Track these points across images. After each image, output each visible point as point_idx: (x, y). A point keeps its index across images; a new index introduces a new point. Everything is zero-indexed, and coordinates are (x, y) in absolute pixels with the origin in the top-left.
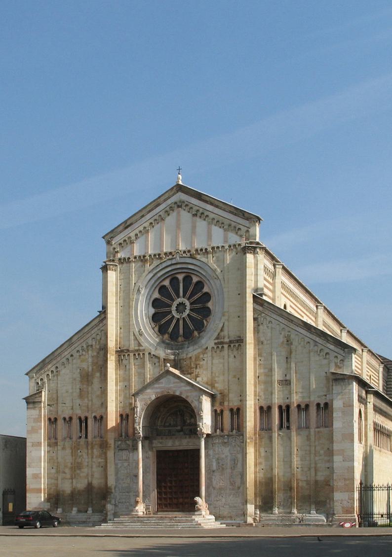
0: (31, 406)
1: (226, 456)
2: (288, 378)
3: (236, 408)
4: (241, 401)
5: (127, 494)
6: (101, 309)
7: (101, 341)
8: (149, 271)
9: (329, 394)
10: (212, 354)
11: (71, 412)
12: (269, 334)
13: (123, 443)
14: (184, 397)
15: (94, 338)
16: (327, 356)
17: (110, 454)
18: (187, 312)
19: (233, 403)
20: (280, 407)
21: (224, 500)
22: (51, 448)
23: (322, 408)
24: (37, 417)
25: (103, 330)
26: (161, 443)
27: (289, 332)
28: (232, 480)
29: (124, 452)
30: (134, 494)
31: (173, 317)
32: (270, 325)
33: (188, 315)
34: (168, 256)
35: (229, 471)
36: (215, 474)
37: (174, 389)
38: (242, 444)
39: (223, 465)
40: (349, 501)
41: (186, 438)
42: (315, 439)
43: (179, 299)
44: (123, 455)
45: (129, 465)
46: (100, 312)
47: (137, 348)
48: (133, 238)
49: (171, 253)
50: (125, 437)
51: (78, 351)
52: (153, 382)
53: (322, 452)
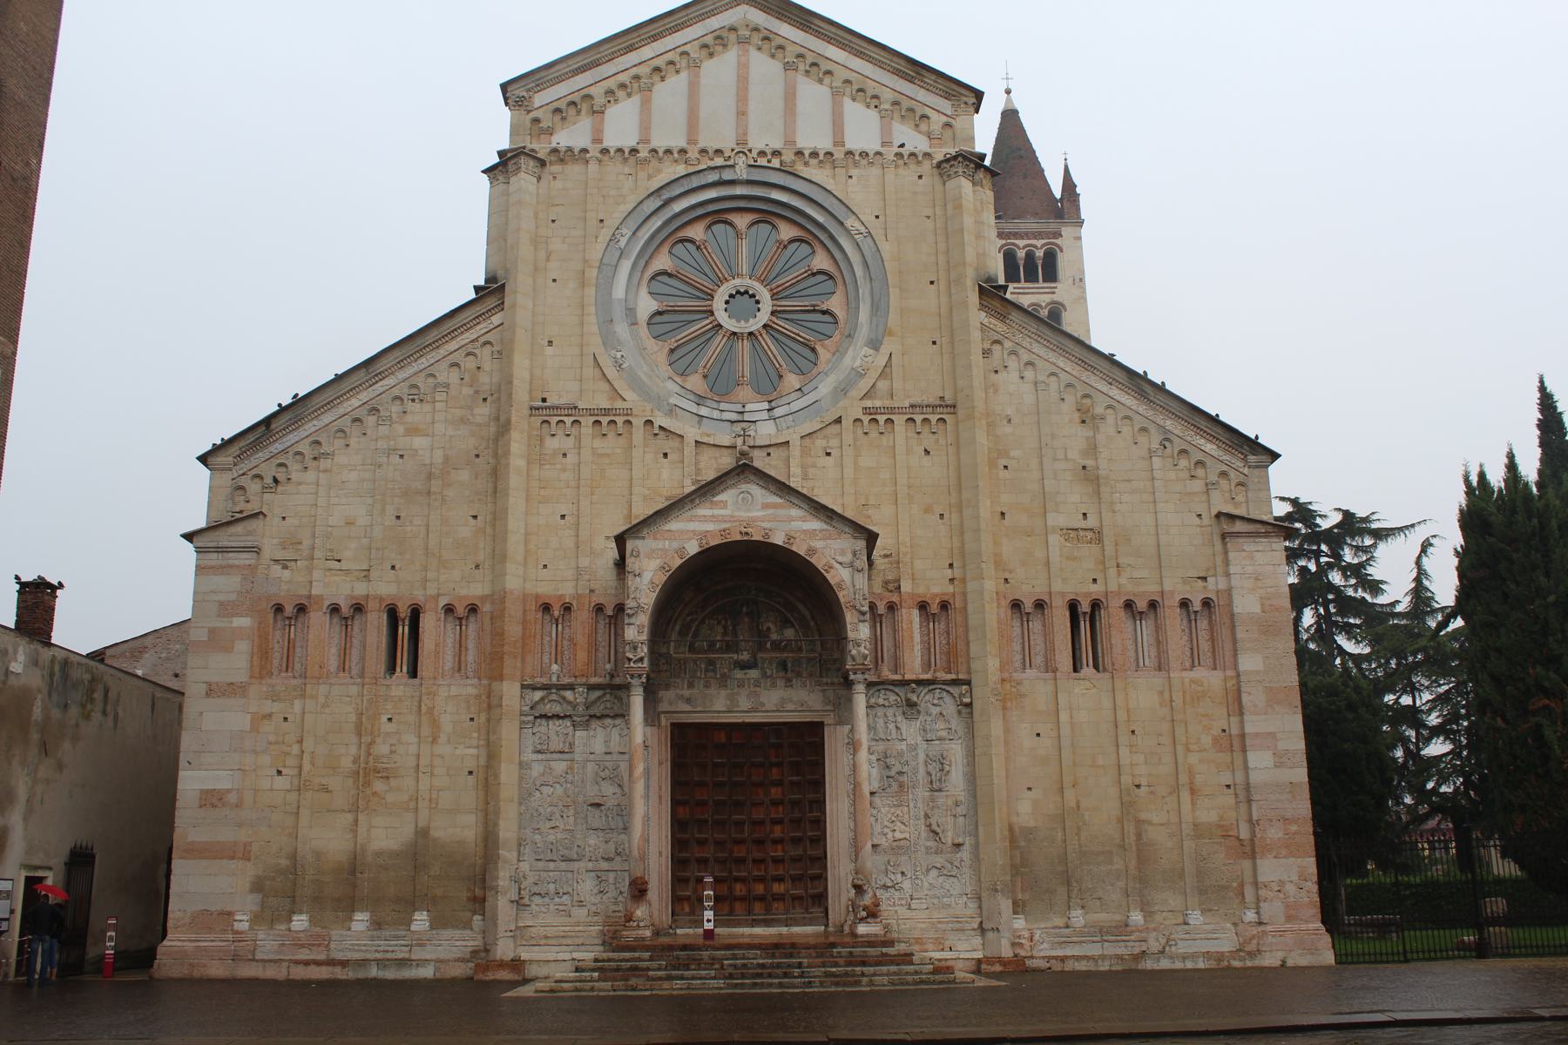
0: (213, 560)
1: (913, 748)
2: (1092, 522)
3: (937, 601)
4: (952, 580)
5: (563, 865)
6: (482, 283)
7: (484, 379)
8: (652, 190)
9: (1215, 575)
10: (855, 440)
11: (361, 589)
12: (1029, 399)
13: (554, 697)
14: (802, 553)
15: (457, 365)
16: (1200, 472)
17: (508, 731)
18: (764, 317)
19: (929, 589)
20: (1073, 607)
21: (907, 885)
22: (275, 707)
23: (1196, 612)
24: (233, 597)
25: (489, 343)
26: (688, 701)
27: (1086, 396)
28: (933, 821)
29: (554, 726)
30: (590, 865)
31: (720, 326)
32: (1029, 374)
33: (765, 326)
34: (712, 159)
35: (922, 793)
36: (877, 800)
37: (766, 525)
38: (965, 710)
39: (901, 773)
40: (1303, 884)
41: (774, 685)
42: (1184, 703)
43: (737, 282)
44: (553, 737)
45: (571, 768)
46: (477, 289)
47: (605, 404)
48: (599, 100)
49: (718, 152)
50: (558, 677)
51: (397, 398)
52: (692, 501)
53: (1207, 740)
